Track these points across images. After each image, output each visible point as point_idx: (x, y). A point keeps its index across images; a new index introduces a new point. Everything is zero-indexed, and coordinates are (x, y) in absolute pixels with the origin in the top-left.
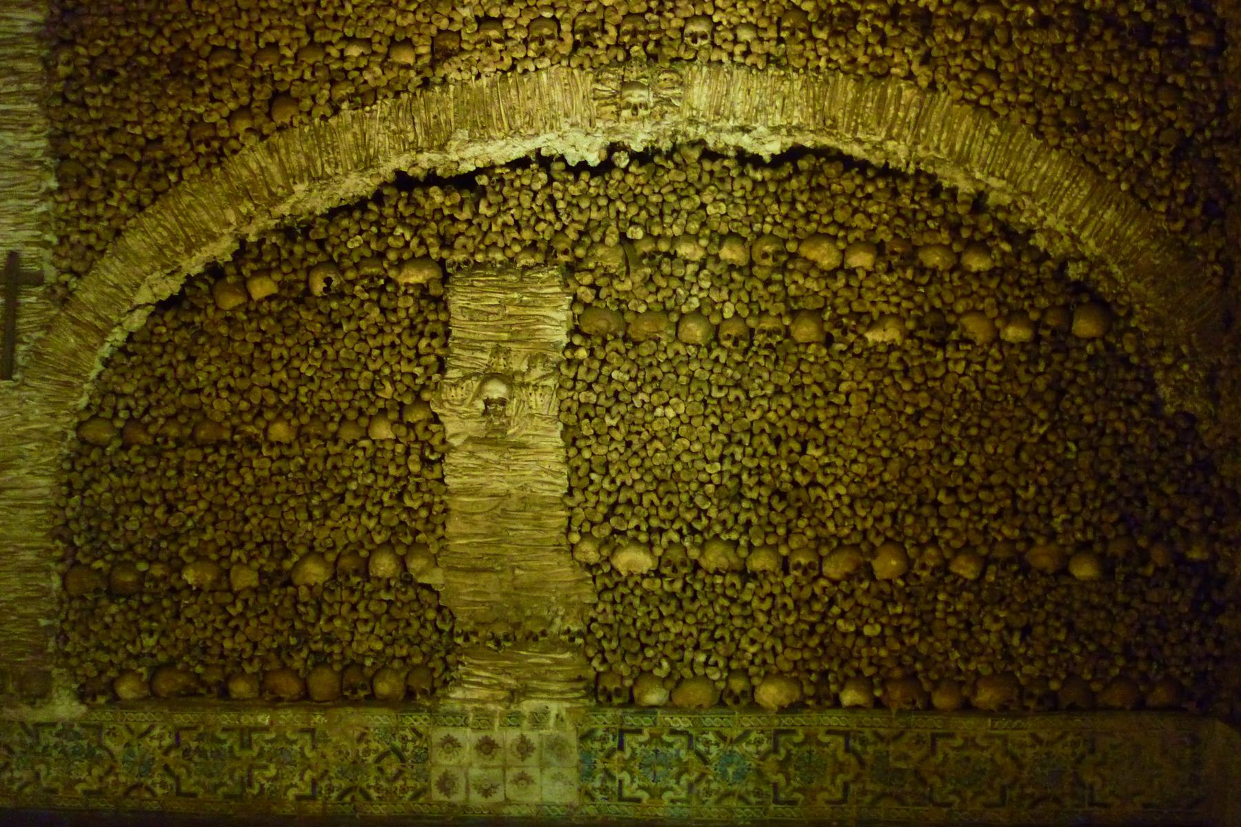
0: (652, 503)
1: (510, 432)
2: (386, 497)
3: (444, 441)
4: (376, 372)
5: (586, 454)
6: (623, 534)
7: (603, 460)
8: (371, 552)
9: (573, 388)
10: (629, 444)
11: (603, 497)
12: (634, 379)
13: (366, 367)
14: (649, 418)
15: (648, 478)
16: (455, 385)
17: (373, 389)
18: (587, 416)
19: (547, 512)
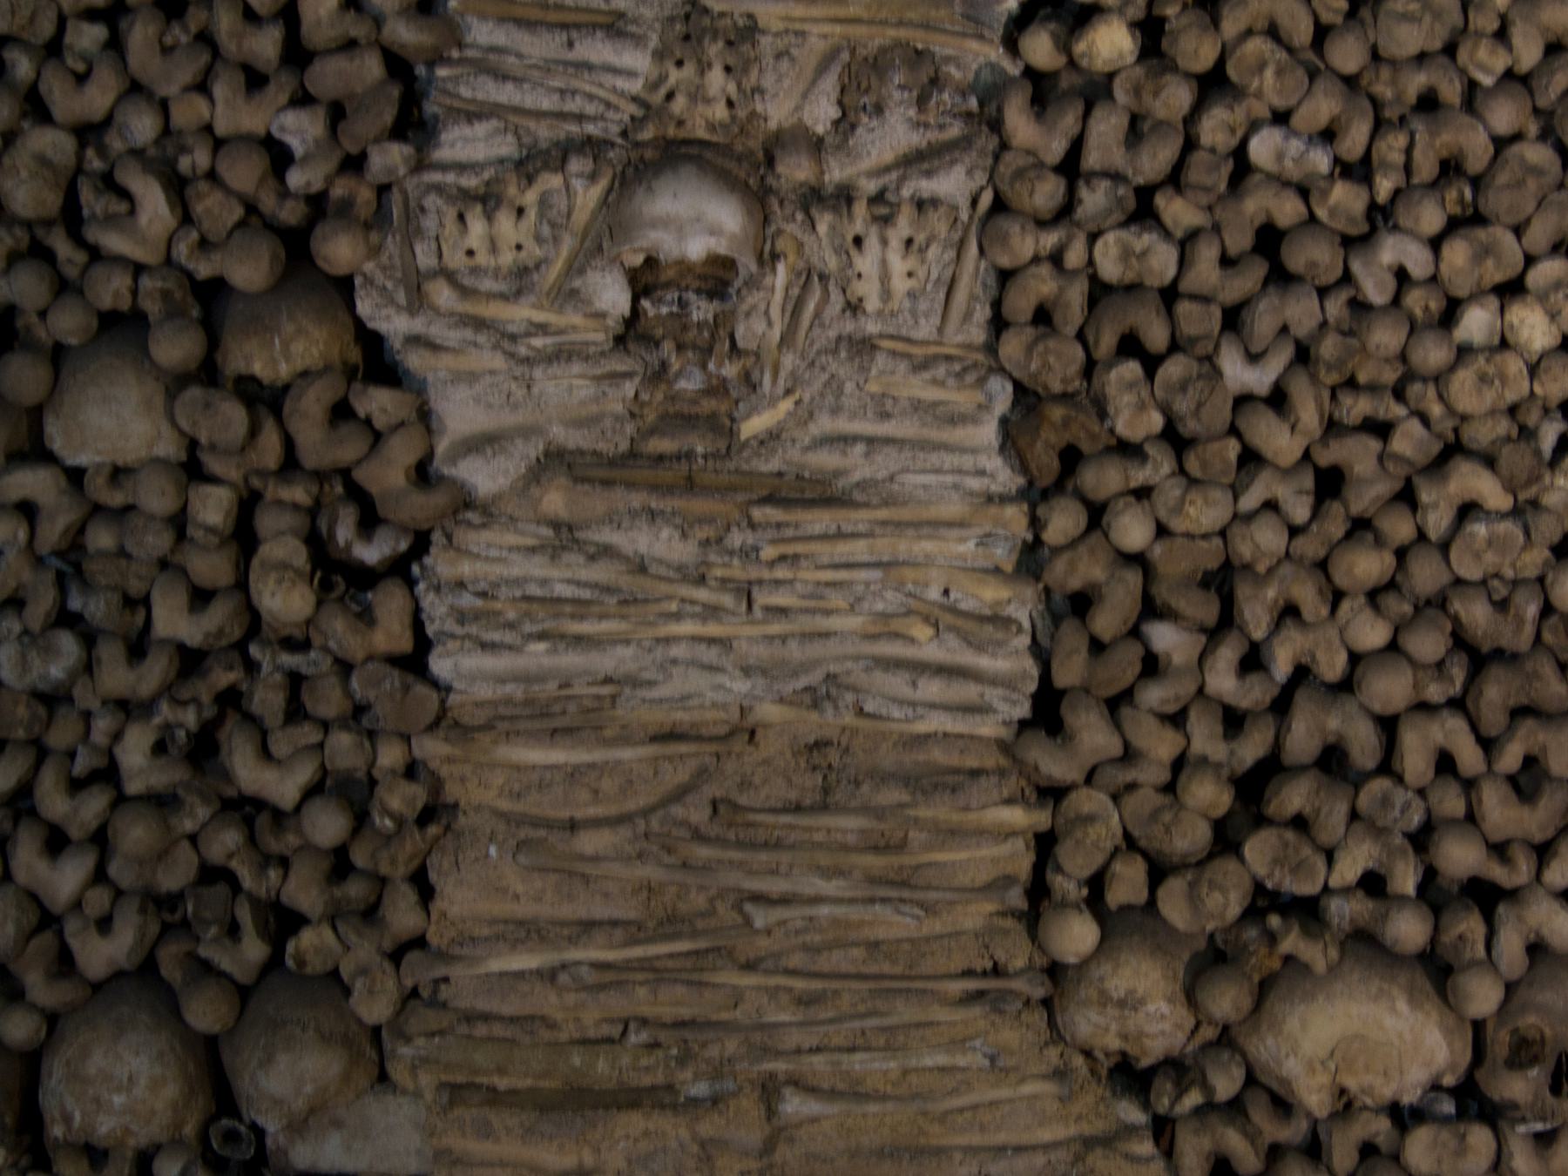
0: (1445, 763)
1: (753, 426)
2: (134, 753)
3: (423, 474)
4: (88, 133)
5: (1133, 531)
6: (1308, 911)
7: (1209, 556)
8: (52, 1020)
9: (1065, 211)
10: (1330, 483)
11: (1205, 737)
12: (1359, 171)
13: (36, 108)
14: (1433, 354)
15: (1428, 644)
16: (489, 200)
17: (72, 217)
18: (1130, 346)
19: (939, 810)
